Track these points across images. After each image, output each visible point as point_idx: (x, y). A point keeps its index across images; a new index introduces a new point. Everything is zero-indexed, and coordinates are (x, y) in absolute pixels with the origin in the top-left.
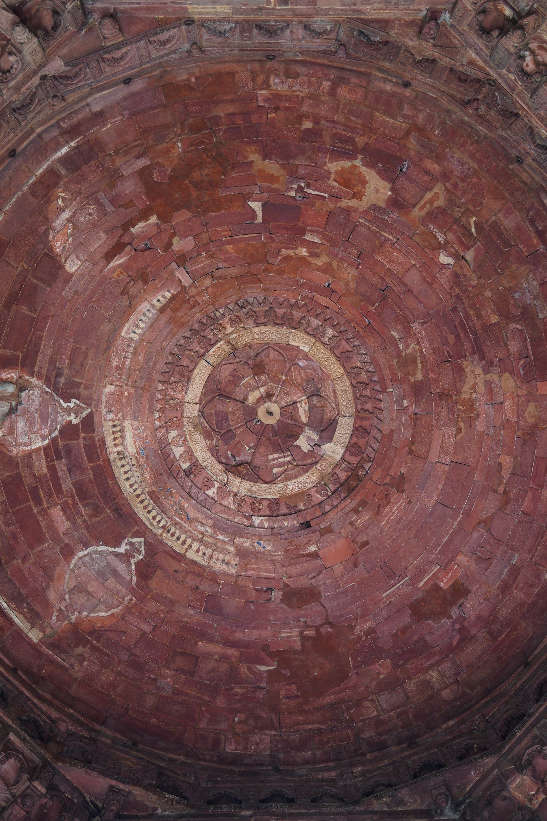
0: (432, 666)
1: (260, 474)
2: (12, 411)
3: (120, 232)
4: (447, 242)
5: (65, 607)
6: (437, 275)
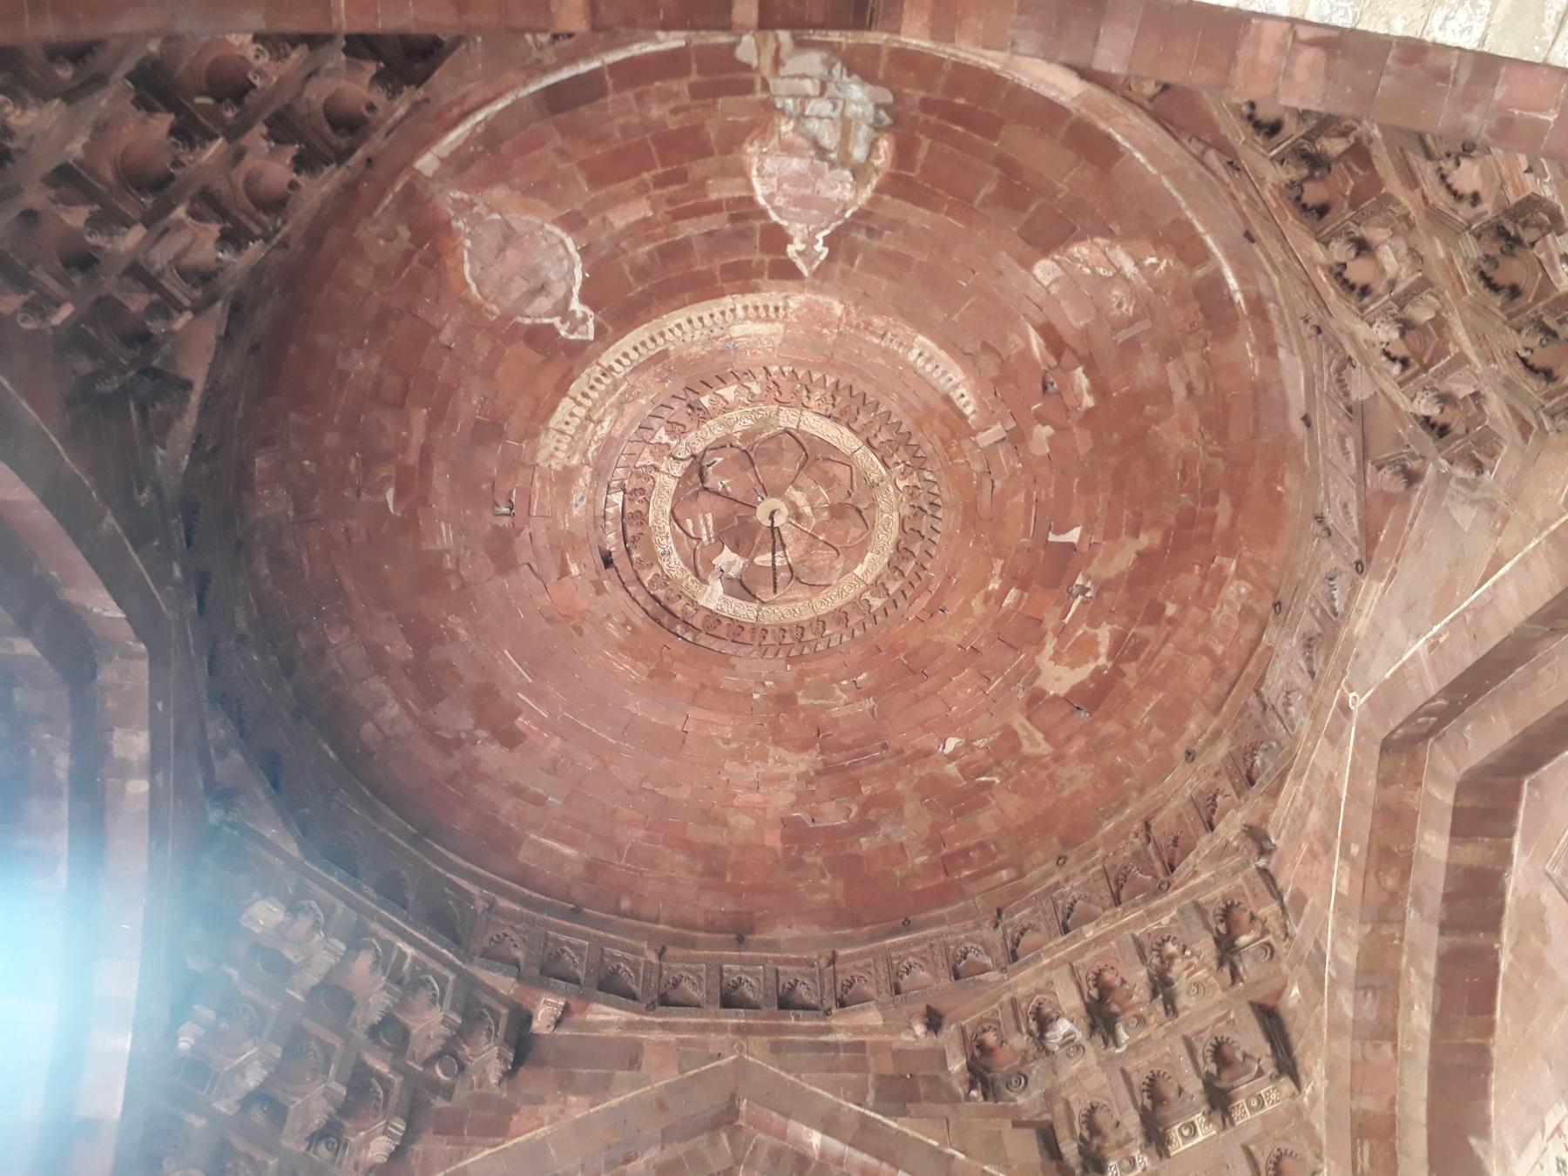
0: (405, 707)
2: (822, 152)
4: (973, 749)
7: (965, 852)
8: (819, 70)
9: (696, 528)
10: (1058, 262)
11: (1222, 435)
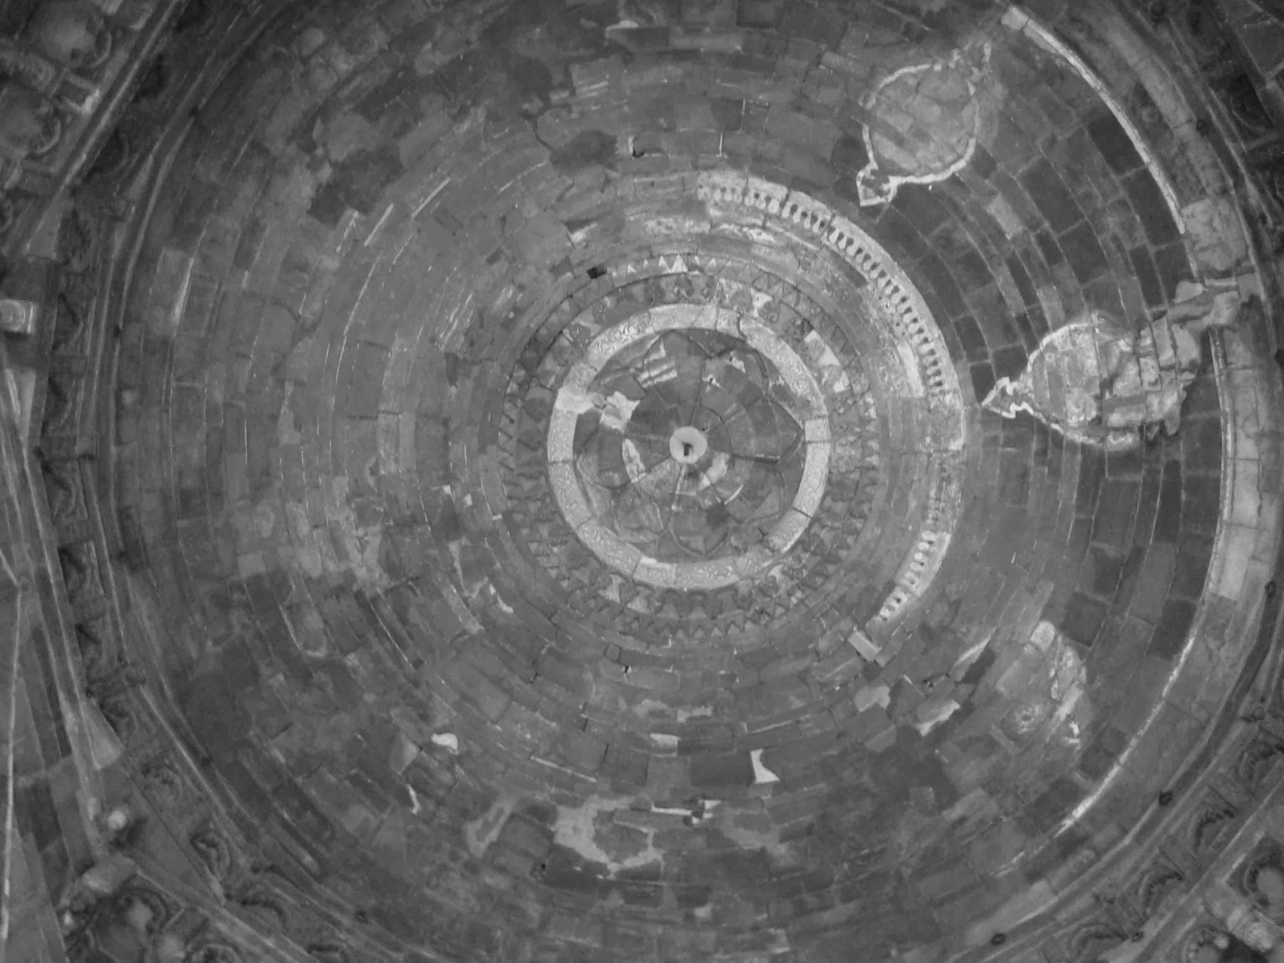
0: (348, 80)
1: (686, 344)
2: (1108, 384)
3: (975, 700)
4: (450, 769)
5: (972, 73)
6: (455, 714)
7: (307, 804)
8: (1185, 361)
9: (657, 363)
10: (1054, 643)
11: (920, 873)
